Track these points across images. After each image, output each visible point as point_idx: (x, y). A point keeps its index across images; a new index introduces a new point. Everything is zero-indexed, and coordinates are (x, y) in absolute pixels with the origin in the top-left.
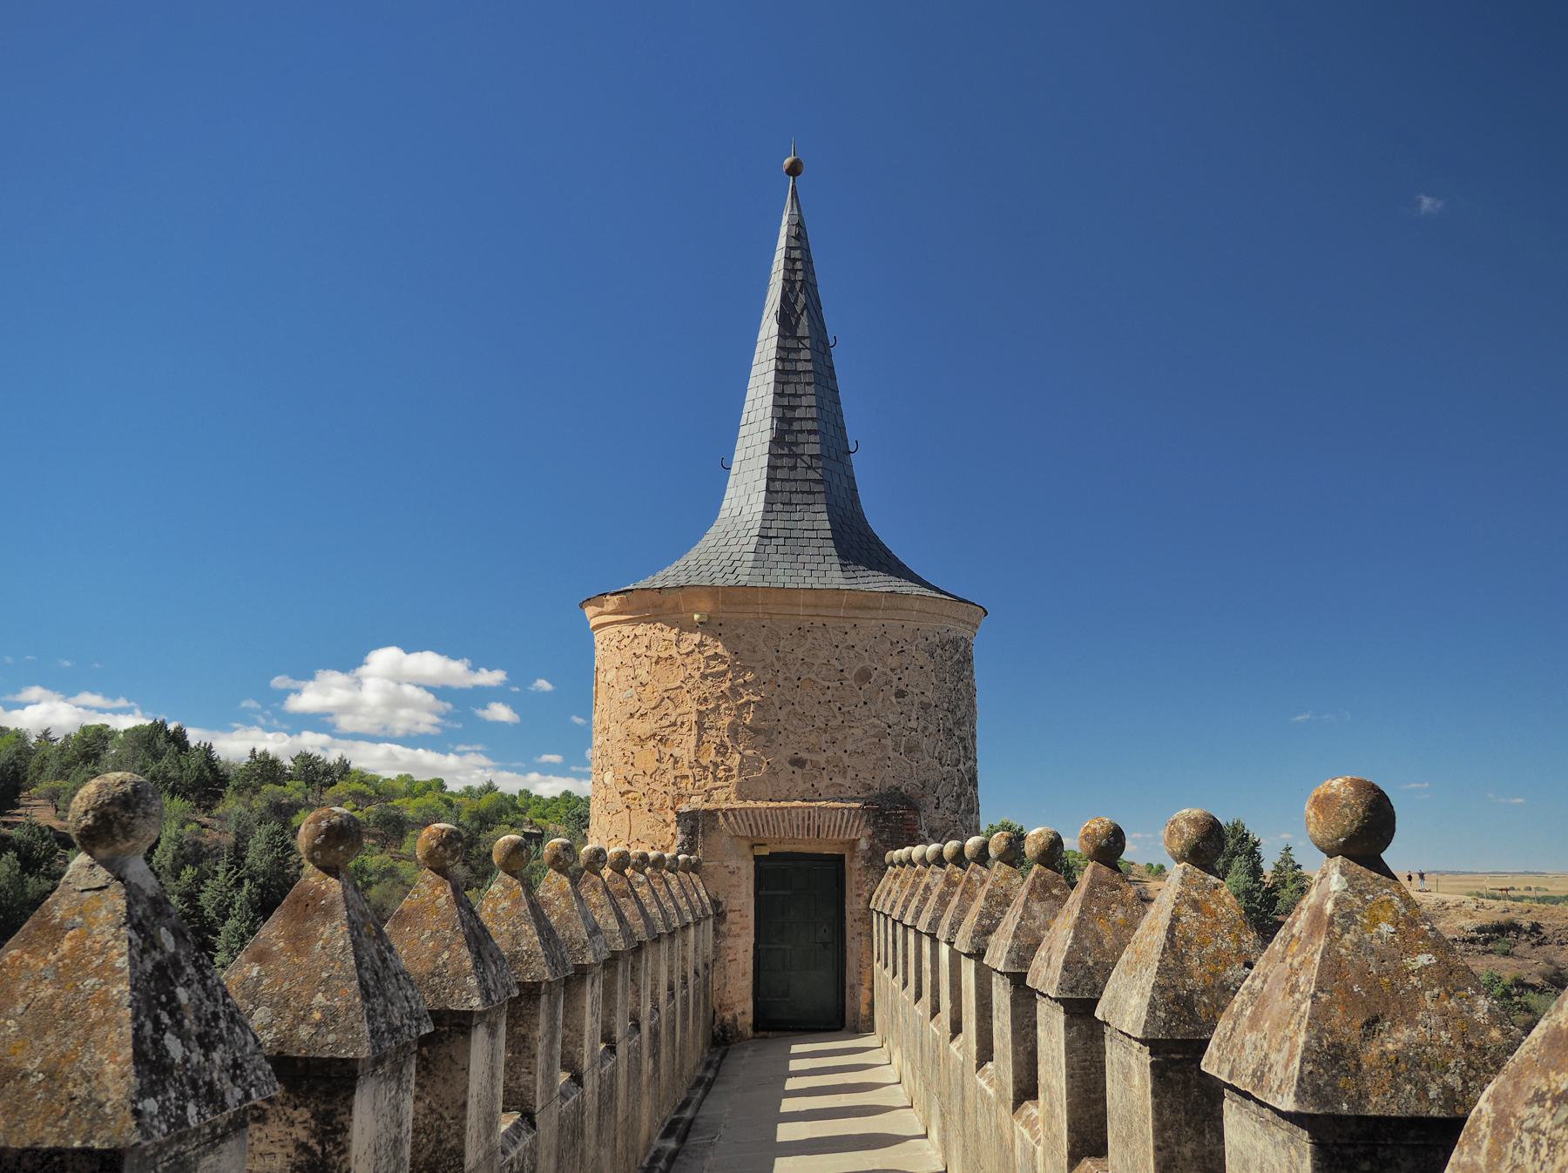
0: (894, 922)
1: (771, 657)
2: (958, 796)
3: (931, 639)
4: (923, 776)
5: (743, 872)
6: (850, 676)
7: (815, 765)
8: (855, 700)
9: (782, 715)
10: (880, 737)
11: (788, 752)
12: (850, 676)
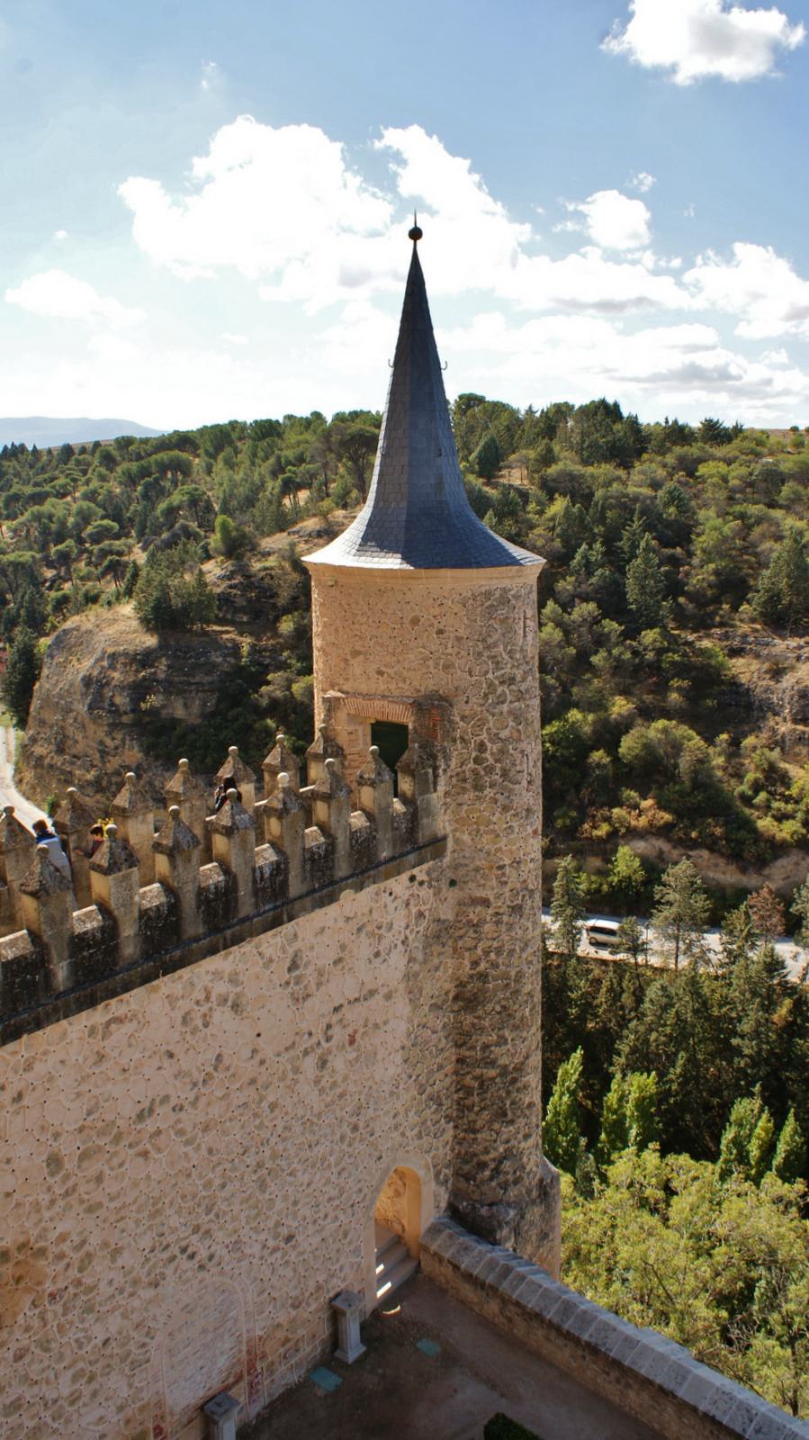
1: (365, 609)
2: (486, 695)
4: (456, 684)
7: (389, 675)
9: (372, 643)
10: (425, 659)
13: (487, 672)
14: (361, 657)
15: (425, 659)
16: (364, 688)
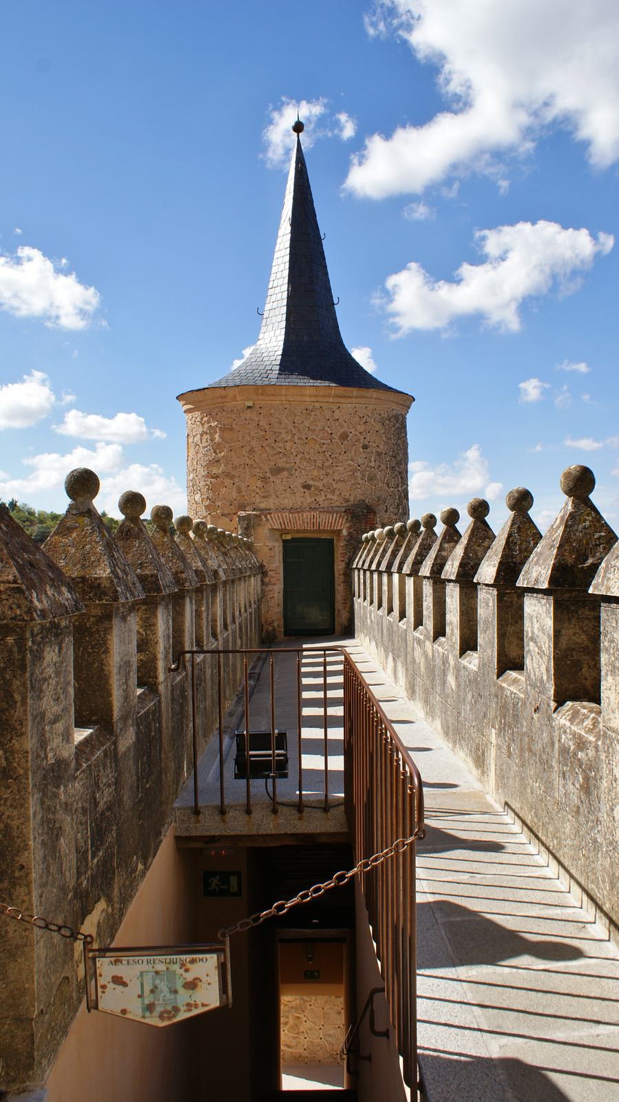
0: (365, 571)
1: (290, 427)
2: (398, 505)
3: (383, 415)
4: (378, 494)
5: (277, 549)
6: (336, 436)
7: (317, 488)
8: (339, 451)
10: (354, 471)
11: (301, 481)
12: (336, 436)
13: (398, 485)
14: (285, 474)
15: (354, 471)
16: (288, 503)
